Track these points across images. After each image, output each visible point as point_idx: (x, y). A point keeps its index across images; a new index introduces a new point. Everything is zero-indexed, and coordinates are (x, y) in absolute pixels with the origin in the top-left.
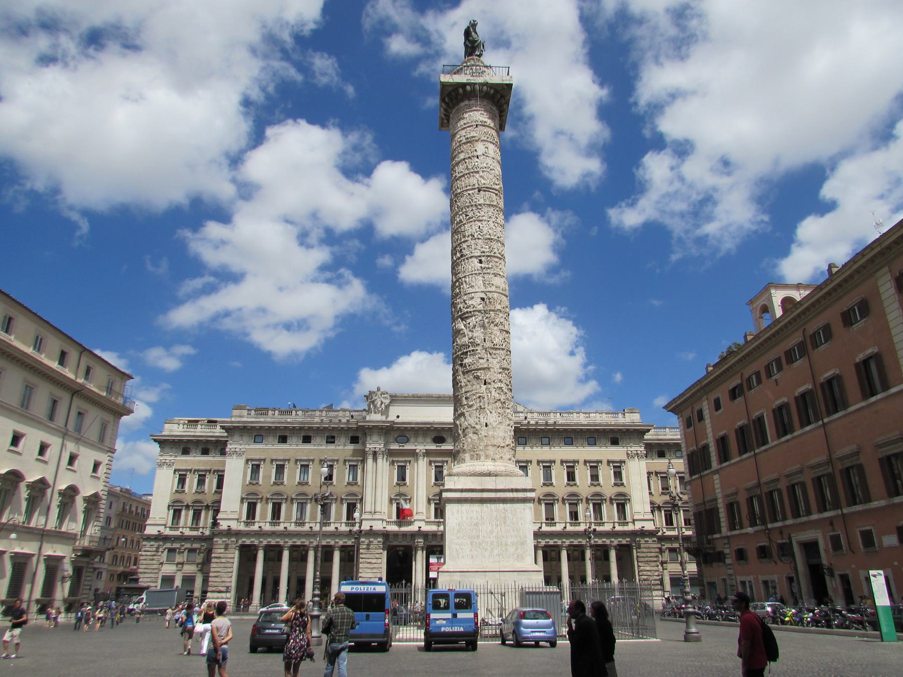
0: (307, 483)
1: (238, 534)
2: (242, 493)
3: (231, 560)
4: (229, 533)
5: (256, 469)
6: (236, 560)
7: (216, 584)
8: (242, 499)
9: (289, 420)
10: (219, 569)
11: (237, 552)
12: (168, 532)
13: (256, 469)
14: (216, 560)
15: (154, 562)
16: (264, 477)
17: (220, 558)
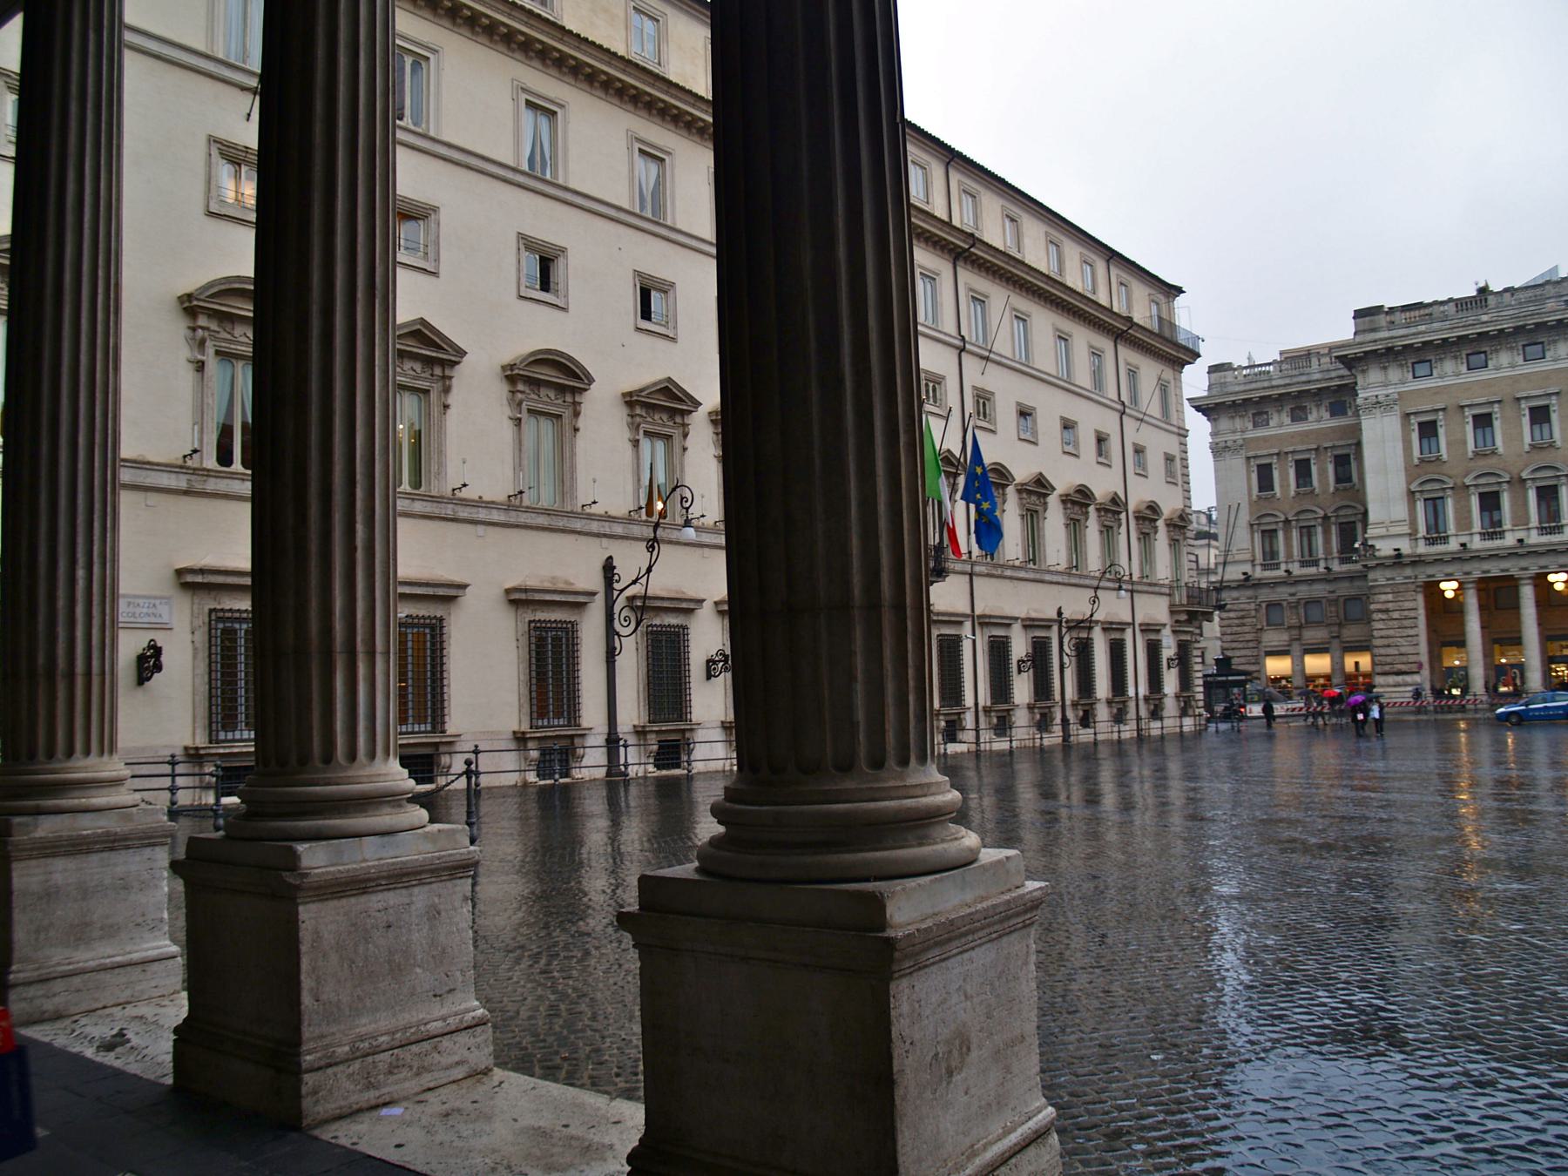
0: (1551, 445)
1: (1418, 561)
2: (1409, 483)
3: (1412, 614)
4: (1398, 559)
5: (1428, 430)
6: (1422, 612)
7: (1389, 659)
8: (1411, 494)
9: (1485, 318)
10: (1391, 632)
11: (1420, 598)
12: (1259, 573)
13: (1428, 430)
14: (1381, 616)
15: (1246, 629)
16: (1448, 444)
17: (1387, 611)
